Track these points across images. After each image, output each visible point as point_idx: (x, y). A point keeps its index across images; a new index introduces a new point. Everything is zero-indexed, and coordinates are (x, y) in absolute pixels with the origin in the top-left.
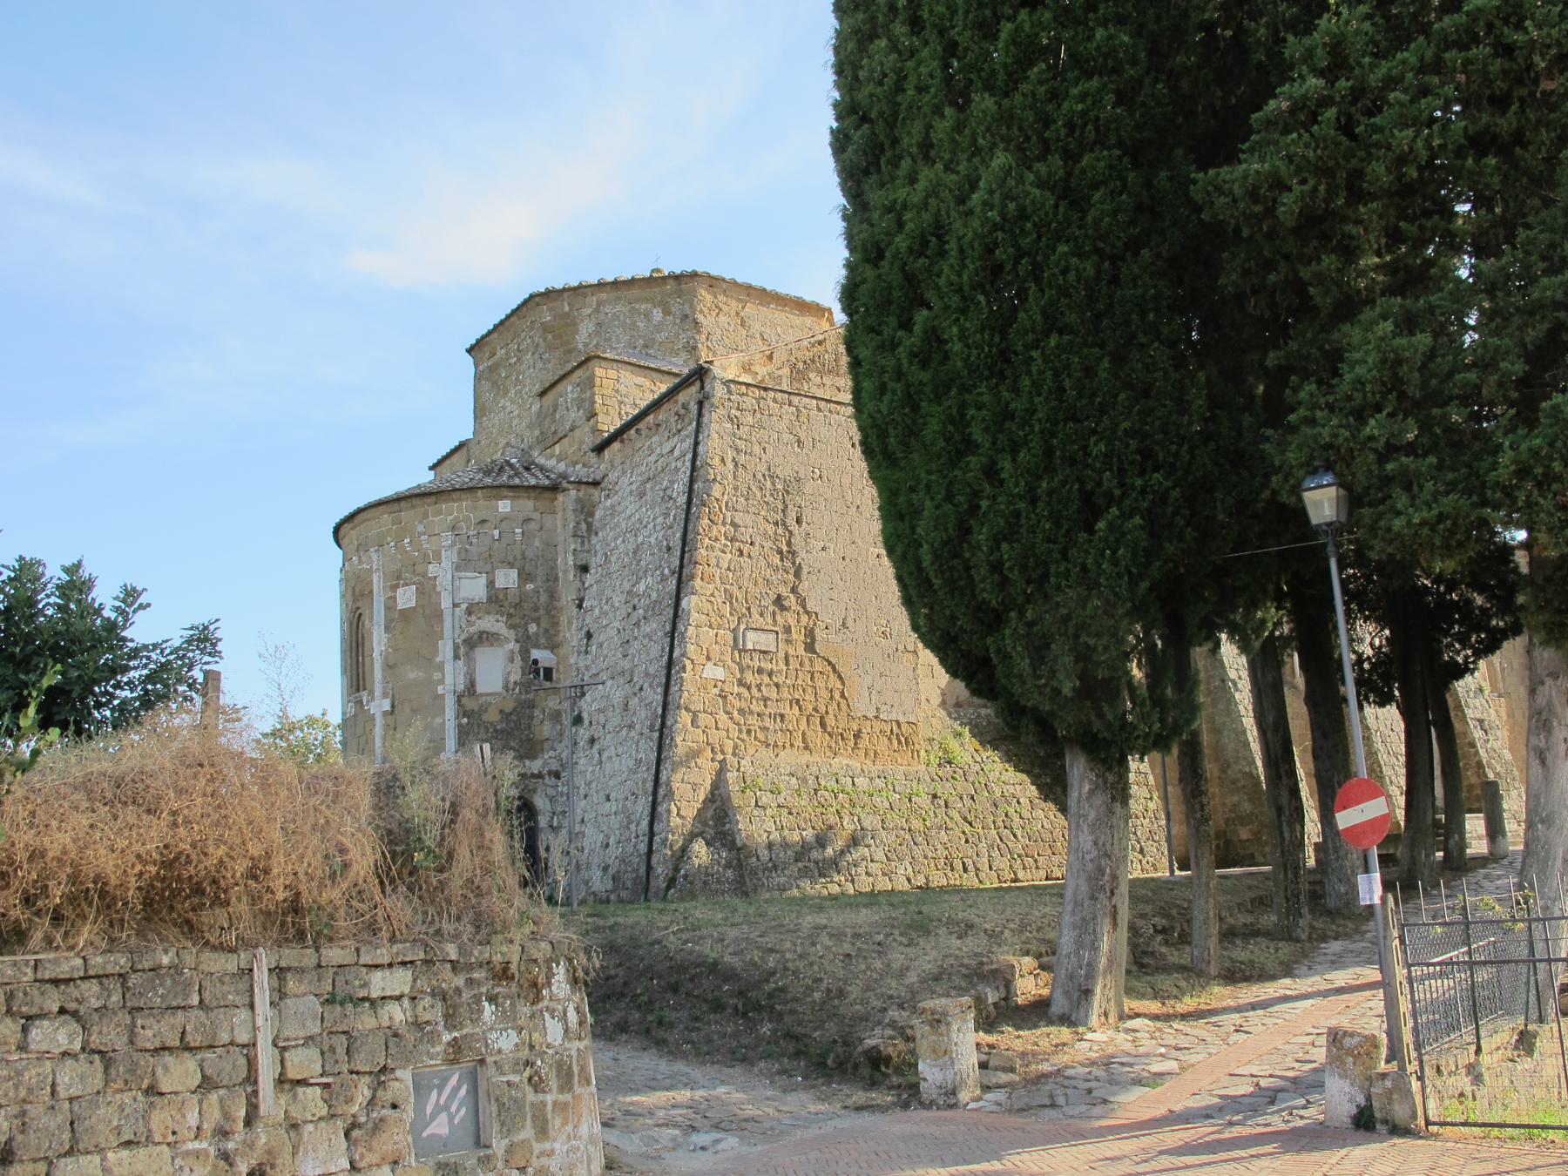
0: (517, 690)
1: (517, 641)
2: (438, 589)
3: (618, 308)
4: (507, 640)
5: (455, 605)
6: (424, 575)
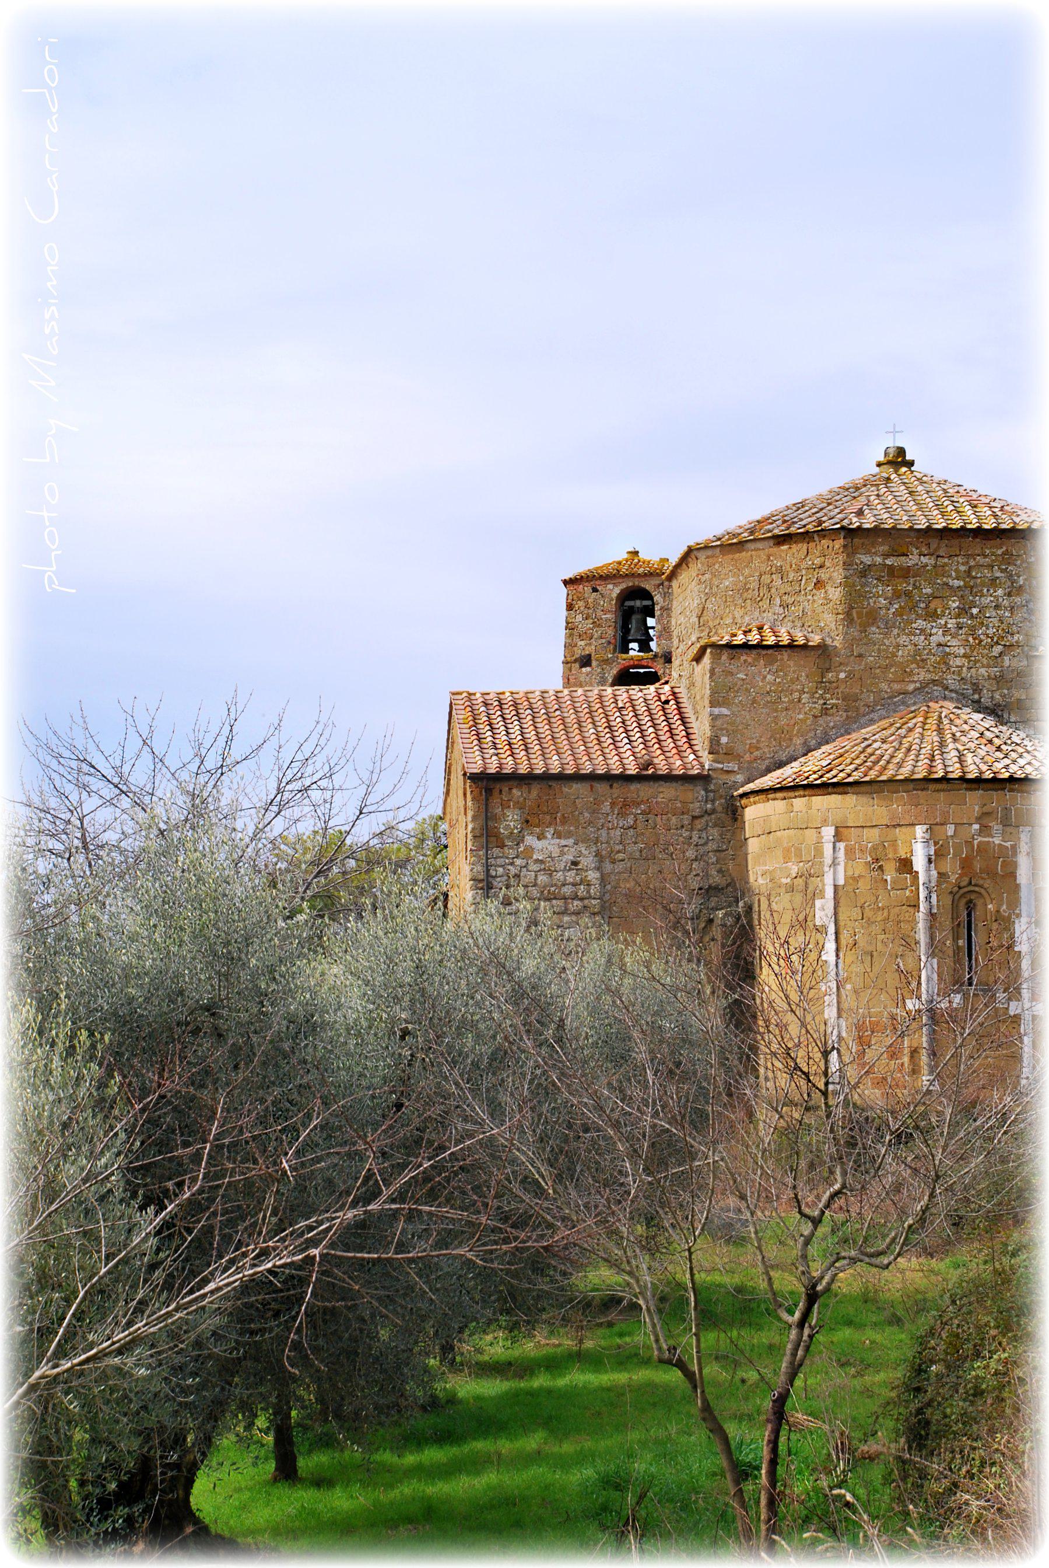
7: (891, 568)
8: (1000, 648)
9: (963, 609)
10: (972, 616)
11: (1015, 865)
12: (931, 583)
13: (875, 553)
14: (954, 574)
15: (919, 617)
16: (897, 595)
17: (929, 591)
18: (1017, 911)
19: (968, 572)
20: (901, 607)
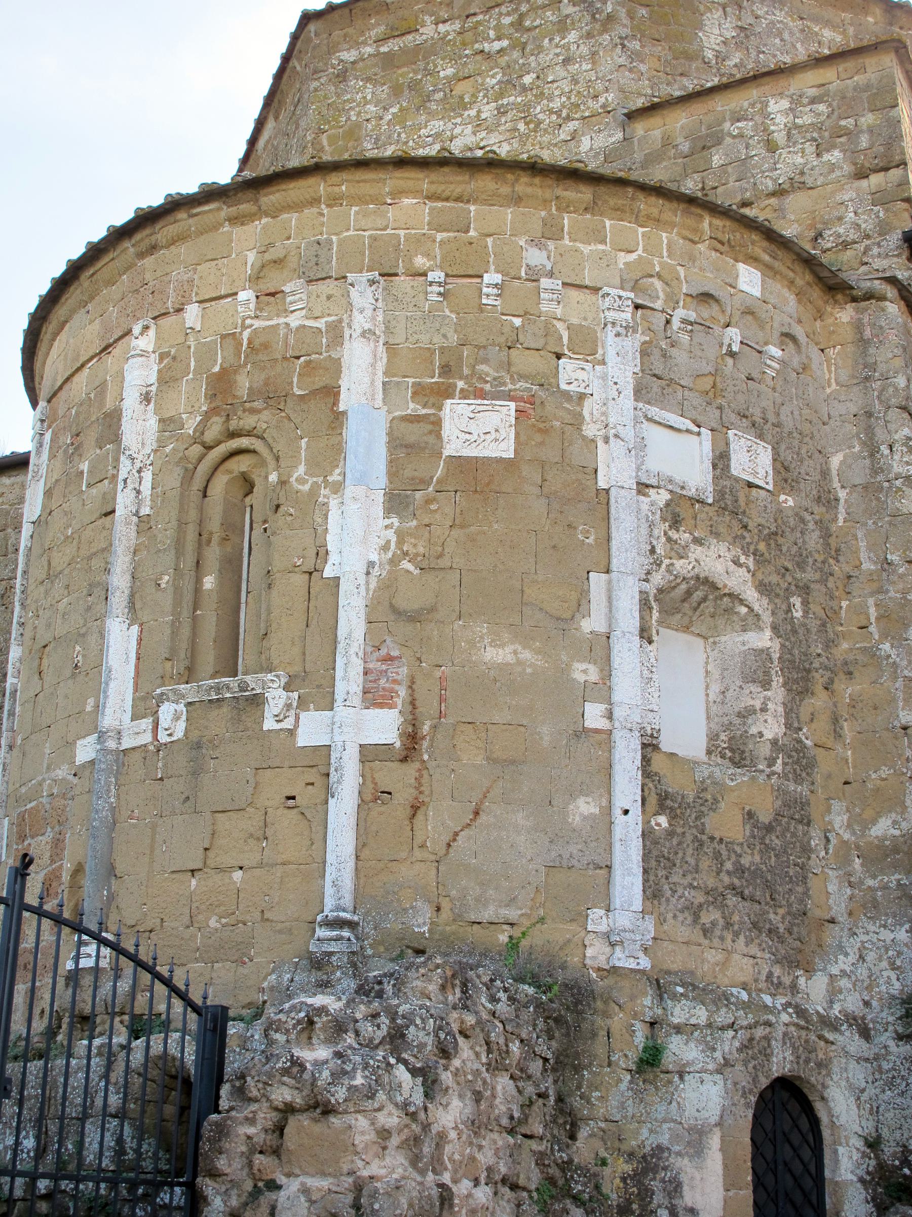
0: (778, 767)
1: (775, 628)
2: (590, 430)
3: (779, 16)
4: (753, 621)
5: (643, 488)
6: (548, 382)
7: (389, 56)
8: (572, 125)
9: (509, 82)
10: (525, 89)
11: (336, 367)
12: (454, 58)
13: (365, 43)
14: (492, 34)
15: (432, 115)
16: (397, 91)
17: (450, 71)
18: (335, 477)
19: (518, 24)
20: (401, 110)
